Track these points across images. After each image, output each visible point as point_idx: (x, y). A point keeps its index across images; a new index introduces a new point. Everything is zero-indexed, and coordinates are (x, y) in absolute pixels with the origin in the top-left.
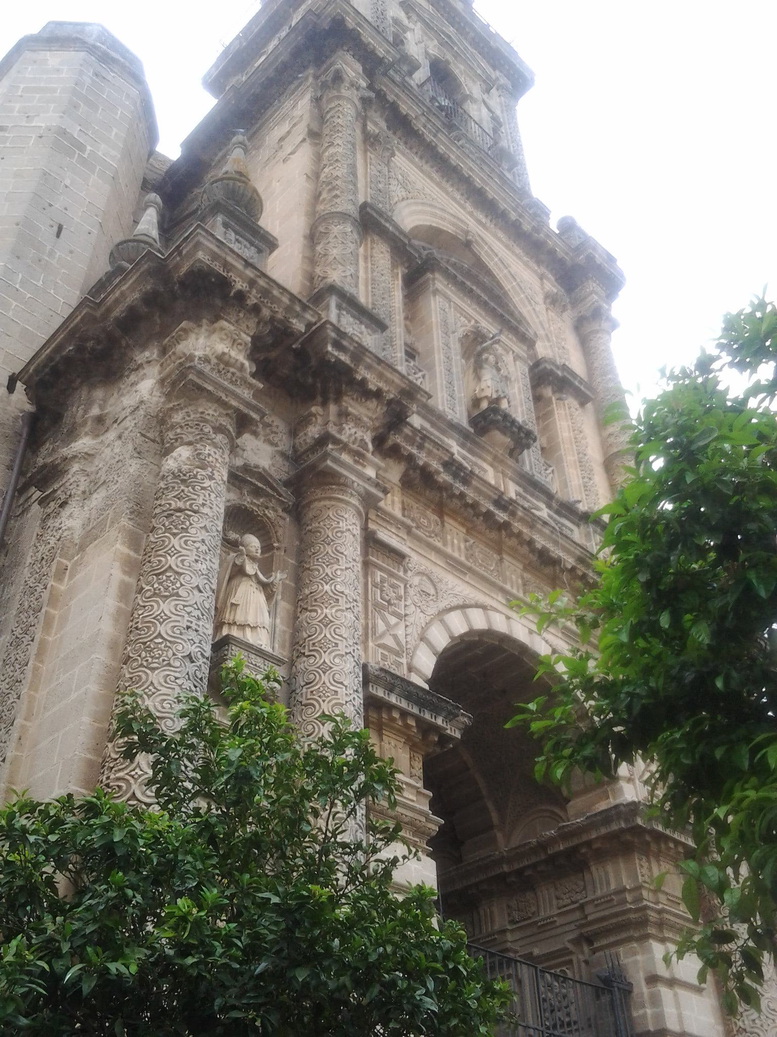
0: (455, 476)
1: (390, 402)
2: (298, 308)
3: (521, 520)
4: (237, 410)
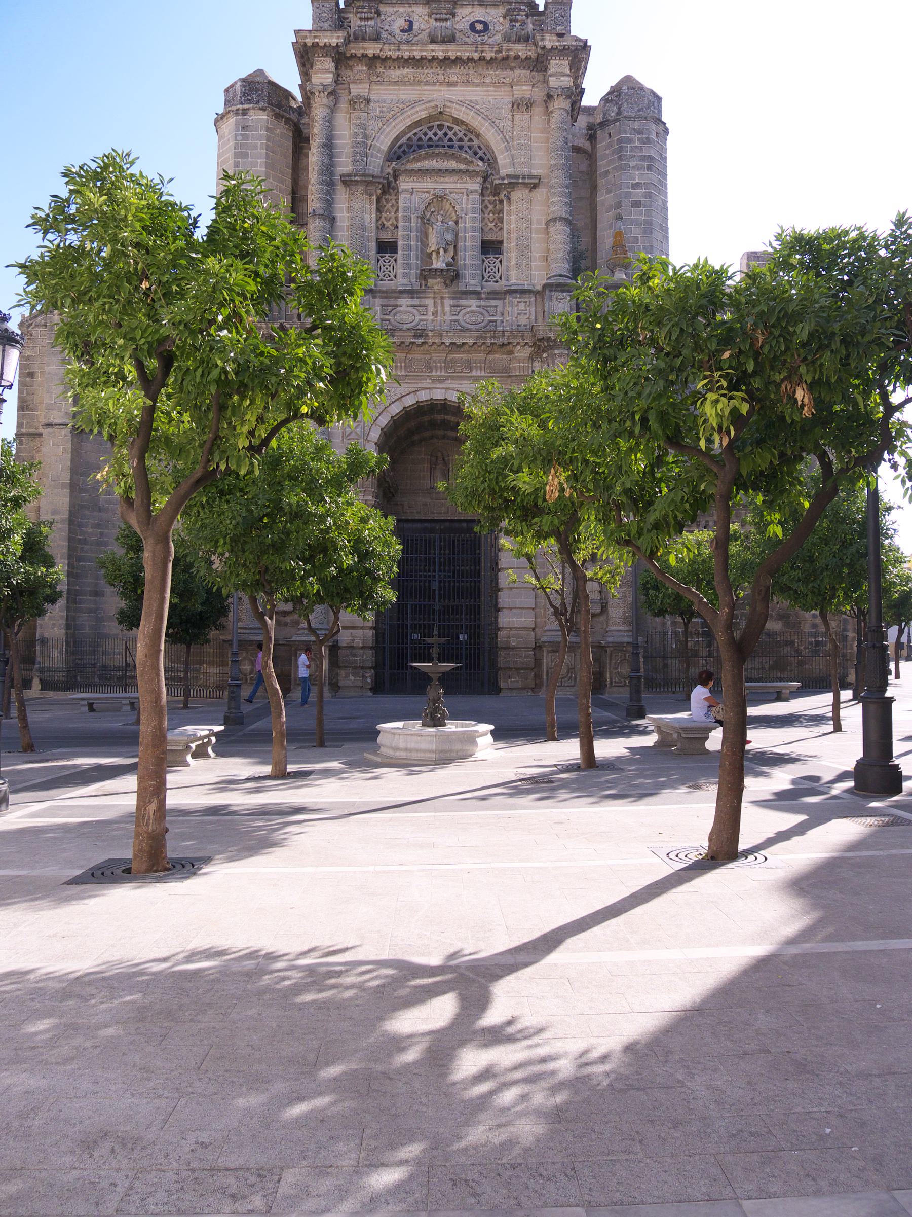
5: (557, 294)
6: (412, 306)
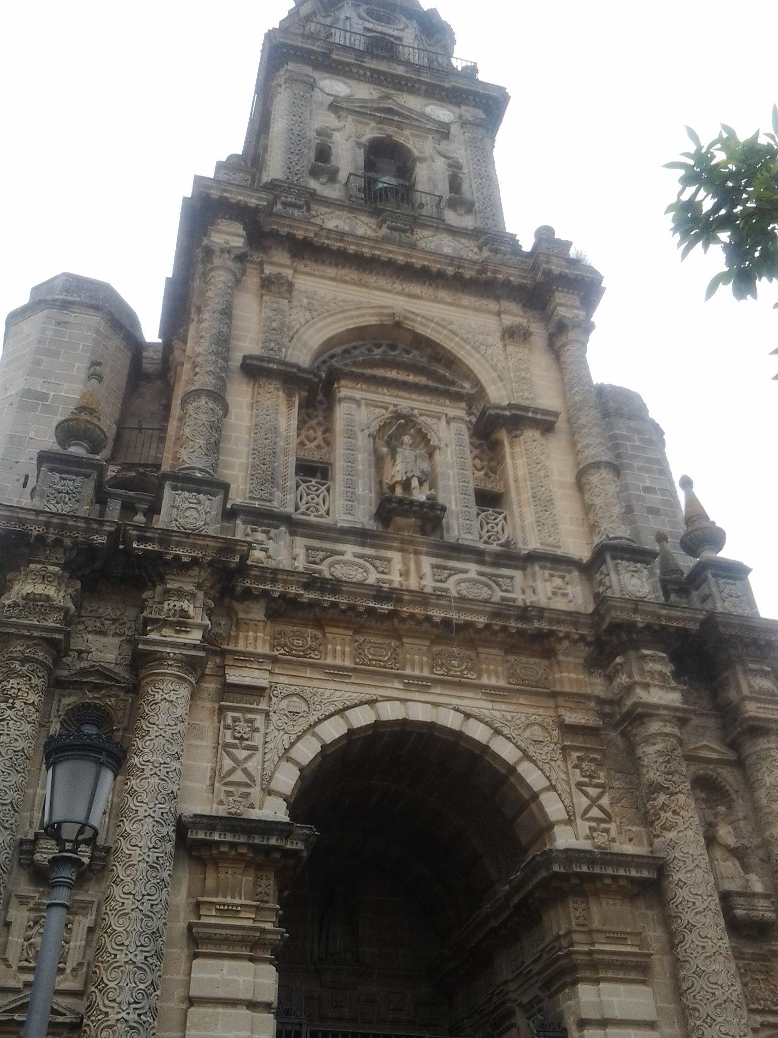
0: (323, 590)
1: (210, 564)
2: (95, 526)
3: (410, 602)
4: (41, 638)
5: (625, 563)
6: (362, 556)
